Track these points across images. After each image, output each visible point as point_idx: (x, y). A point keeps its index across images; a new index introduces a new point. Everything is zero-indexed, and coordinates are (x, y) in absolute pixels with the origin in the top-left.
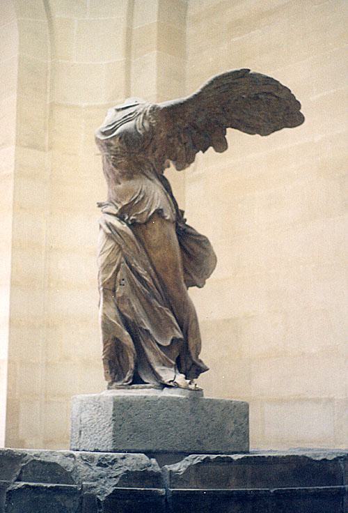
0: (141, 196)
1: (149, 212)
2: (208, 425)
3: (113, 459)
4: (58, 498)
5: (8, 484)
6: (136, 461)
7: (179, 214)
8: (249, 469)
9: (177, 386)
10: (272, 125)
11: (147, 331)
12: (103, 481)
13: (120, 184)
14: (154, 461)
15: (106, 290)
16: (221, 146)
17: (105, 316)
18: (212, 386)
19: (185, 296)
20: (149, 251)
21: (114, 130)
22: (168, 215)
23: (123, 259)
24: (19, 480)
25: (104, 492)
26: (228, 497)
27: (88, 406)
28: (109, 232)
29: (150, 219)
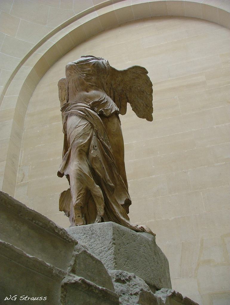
1: (112, 111)
3: (128, 276)
5: (64, 274)
13: (88, 92)
15: (82, 151)
17: (80, 170)
24: (73, 271)
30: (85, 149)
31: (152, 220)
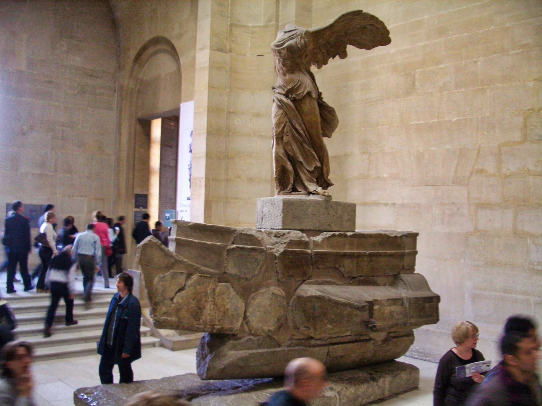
0: (299, 84)
2: (334, 216)
4: (253, 254)
6: (296, 235)
7: (320, 94)
8: (356, 241)
9: (318, 194)
10: (373, 44)
11: (301, 162)
12: (277, 245)
14: (304, 235)
16: (344, 55)
17: (277, 153)
18: (335, 193)
19: (322, 141)
20: (303, 116)
21: (283, 44)
22: (314, 95)
23: (288, 121)
24: (233, 243)
25: (278, 251)
26: (345, 255)
27: (267, 204)
28: (279, 103)
29: (304, 97)
30: (280, 136)
31: (436, 120)
